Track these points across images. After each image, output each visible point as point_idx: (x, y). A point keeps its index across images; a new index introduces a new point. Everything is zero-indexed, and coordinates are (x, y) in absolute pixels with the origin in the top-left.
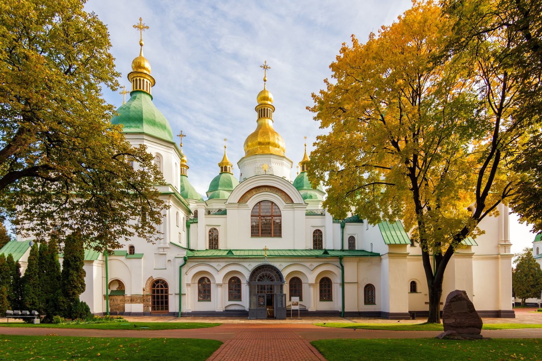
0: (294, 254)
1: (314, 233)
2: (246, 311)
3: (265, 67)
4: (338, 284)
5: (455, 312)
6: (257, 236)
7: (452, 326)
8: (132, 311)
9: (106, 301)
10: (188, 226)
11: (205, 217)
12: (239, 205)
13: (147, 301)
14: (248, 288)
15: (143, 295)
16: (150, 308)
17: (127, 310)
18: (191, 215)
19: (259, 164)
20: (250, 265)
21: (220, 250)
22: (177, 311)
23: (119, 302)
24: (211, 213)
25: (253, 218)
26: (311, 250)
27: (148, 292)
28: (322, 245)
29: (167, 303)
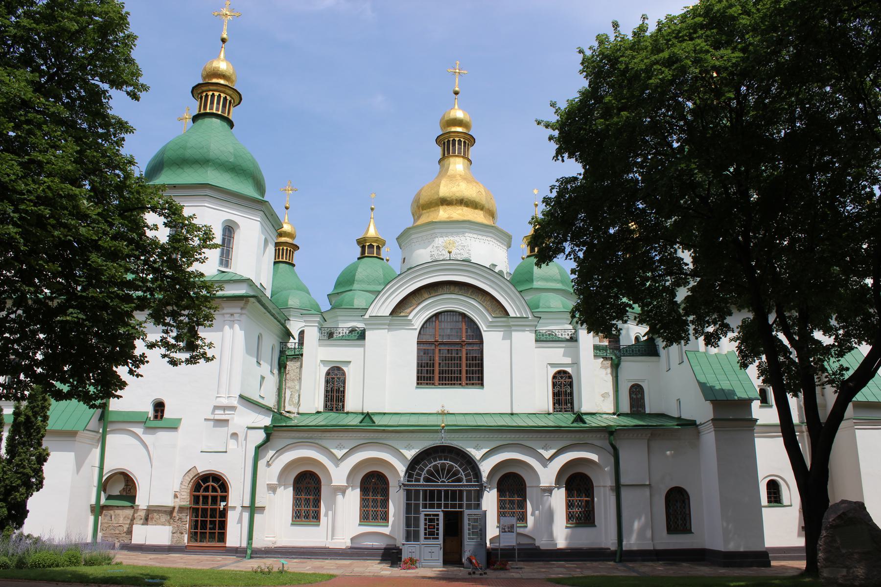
1: (554, 377)
4: (608, 489)
8: (147, 543)
12: (391, 320)
16: (186, 537)
18: (292, 340)
21: (347, 413)
27: (185, 499)
29: (223, 525)
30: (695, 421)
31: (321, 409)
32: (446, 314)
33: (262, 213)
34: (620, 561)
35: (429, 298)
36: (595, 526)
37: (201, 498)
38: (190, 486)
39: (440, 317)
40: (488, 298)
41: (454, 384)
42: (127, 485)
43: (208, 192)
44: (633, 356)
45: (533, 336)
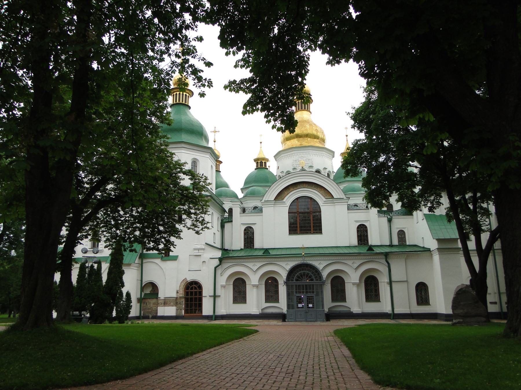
1: (358, 228)
4: (386, 283)
8: (165, 315)
9: (139, 304)
10: (222, 227)
11: (240, 216)
12: (275, 202)
13: (180, 303)
14: (285, 287)
15: (177, 298)
16: (183, 311)
17: (160, 314)
22: (211, 313)
26: (357, 246)
27: (182, 294)
28: (368, 241)
29: (200, 305)
30: (430, 249)
31: (243, 247)
32: (302, 198)
33: (209, 153)
34: (393, 319)
35: (293, 190)
36: (380, 302)
37: (189, 293)
38: (184, 287)
39: (299, 200)
40: (323, 189)
41: (308, 233)
42: (153, 288)
43: (183, 145)
44: (399, 216)
45: (346, 207)
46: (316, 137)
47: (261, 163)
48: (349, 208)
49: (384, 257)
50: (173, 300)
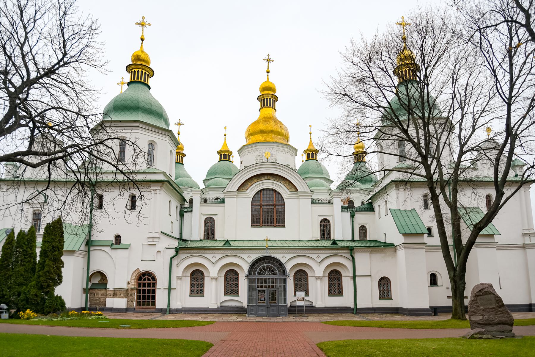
0: (299, 244)
1: (321, 222)
2: (244, 308)
3: (268, 60)
5: (481, 307)
6: (258, 226)
7: (479, 324)
8: (114, 307)
10: (182, 215)
12: (238, 193)
13: (131, 295)
16: (135, 303)
17: (108, 305)
19: (261, 151)
20: (249, 256)
21: (216, 240)
22: (165, 306)
23: (100, 296)
24: (208, 202)
25: (254, 206)
26: (318, 240)
27: (133, 285)
29: (154, 298)
40: (287, 182)
42: (102, 278)
46: (279, 134)
47: (225, 155)
48: (314, 202)
49: (349, 251)
50: (123, 291)
